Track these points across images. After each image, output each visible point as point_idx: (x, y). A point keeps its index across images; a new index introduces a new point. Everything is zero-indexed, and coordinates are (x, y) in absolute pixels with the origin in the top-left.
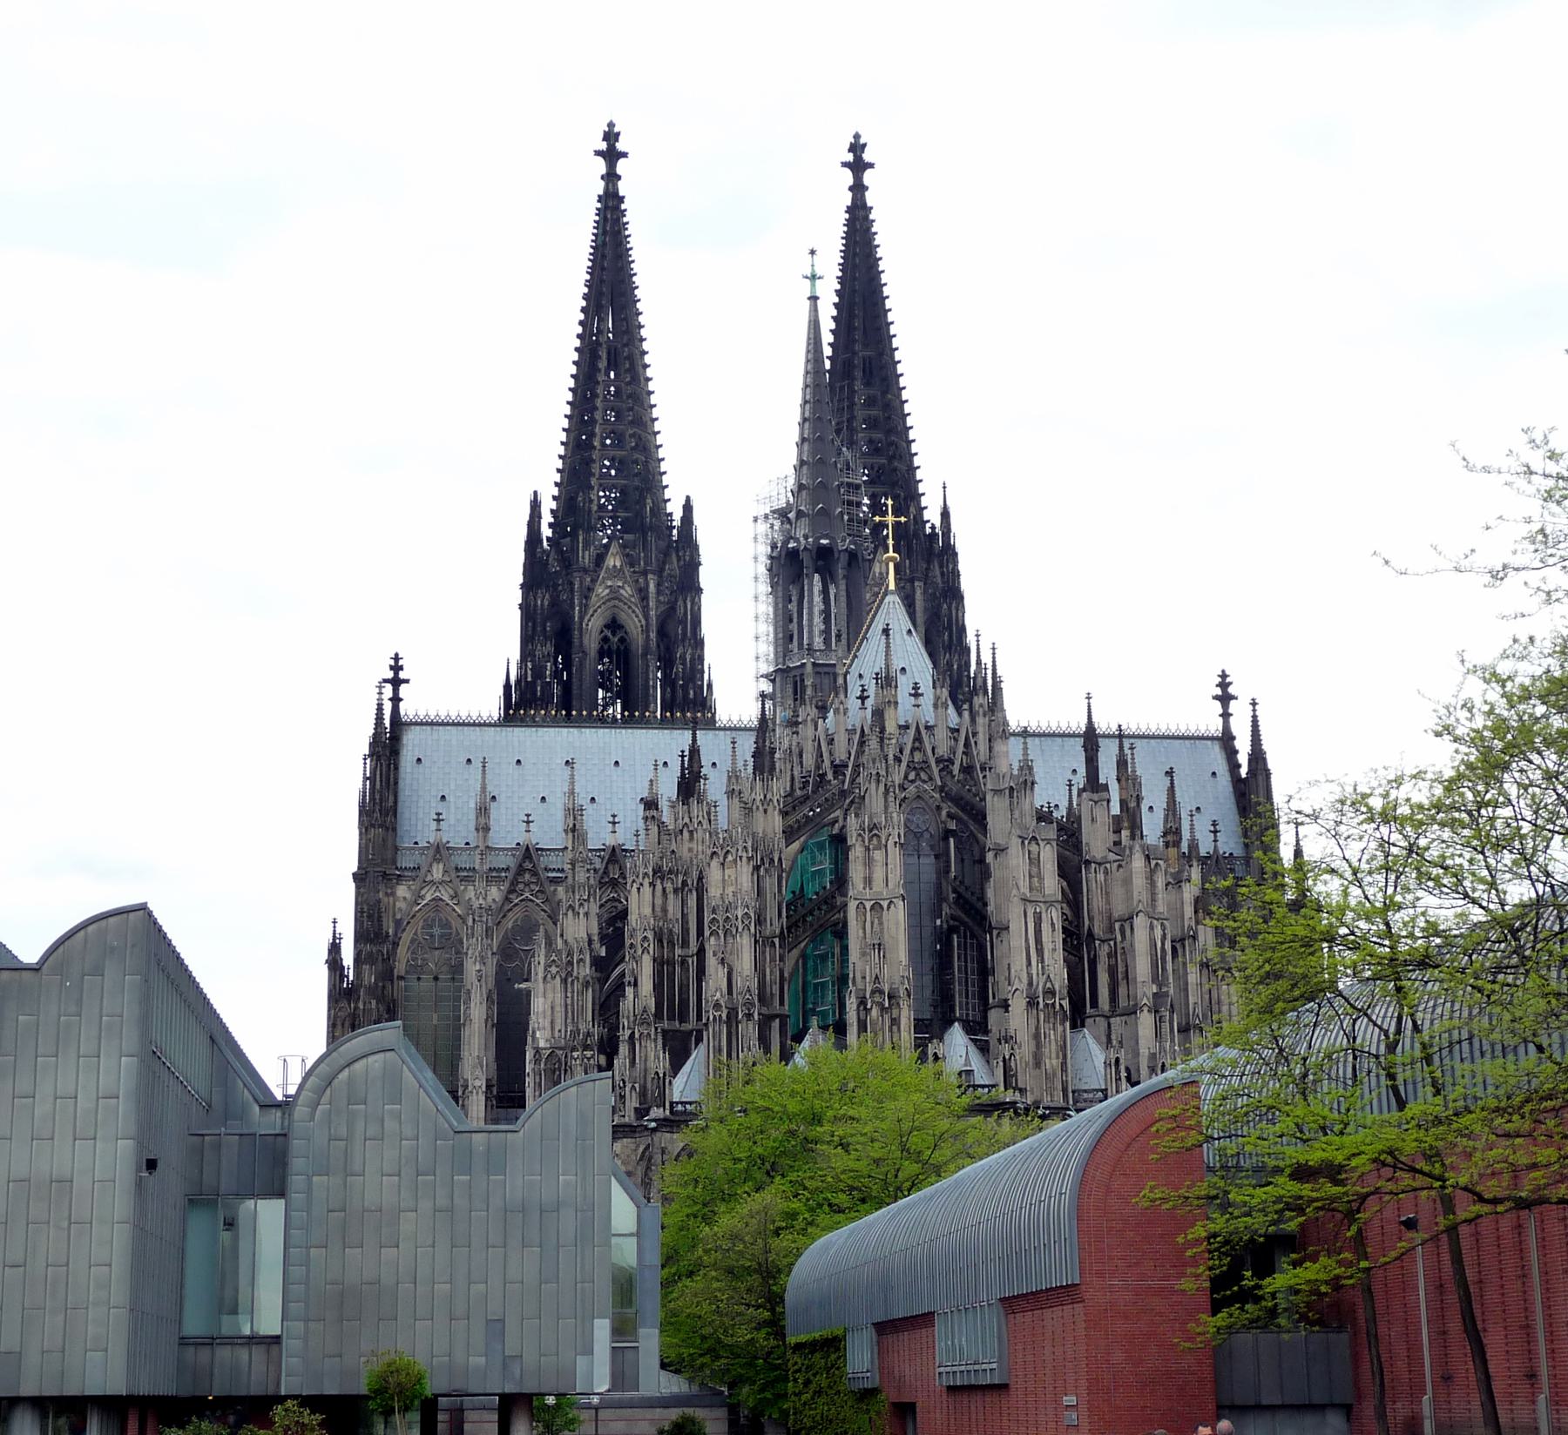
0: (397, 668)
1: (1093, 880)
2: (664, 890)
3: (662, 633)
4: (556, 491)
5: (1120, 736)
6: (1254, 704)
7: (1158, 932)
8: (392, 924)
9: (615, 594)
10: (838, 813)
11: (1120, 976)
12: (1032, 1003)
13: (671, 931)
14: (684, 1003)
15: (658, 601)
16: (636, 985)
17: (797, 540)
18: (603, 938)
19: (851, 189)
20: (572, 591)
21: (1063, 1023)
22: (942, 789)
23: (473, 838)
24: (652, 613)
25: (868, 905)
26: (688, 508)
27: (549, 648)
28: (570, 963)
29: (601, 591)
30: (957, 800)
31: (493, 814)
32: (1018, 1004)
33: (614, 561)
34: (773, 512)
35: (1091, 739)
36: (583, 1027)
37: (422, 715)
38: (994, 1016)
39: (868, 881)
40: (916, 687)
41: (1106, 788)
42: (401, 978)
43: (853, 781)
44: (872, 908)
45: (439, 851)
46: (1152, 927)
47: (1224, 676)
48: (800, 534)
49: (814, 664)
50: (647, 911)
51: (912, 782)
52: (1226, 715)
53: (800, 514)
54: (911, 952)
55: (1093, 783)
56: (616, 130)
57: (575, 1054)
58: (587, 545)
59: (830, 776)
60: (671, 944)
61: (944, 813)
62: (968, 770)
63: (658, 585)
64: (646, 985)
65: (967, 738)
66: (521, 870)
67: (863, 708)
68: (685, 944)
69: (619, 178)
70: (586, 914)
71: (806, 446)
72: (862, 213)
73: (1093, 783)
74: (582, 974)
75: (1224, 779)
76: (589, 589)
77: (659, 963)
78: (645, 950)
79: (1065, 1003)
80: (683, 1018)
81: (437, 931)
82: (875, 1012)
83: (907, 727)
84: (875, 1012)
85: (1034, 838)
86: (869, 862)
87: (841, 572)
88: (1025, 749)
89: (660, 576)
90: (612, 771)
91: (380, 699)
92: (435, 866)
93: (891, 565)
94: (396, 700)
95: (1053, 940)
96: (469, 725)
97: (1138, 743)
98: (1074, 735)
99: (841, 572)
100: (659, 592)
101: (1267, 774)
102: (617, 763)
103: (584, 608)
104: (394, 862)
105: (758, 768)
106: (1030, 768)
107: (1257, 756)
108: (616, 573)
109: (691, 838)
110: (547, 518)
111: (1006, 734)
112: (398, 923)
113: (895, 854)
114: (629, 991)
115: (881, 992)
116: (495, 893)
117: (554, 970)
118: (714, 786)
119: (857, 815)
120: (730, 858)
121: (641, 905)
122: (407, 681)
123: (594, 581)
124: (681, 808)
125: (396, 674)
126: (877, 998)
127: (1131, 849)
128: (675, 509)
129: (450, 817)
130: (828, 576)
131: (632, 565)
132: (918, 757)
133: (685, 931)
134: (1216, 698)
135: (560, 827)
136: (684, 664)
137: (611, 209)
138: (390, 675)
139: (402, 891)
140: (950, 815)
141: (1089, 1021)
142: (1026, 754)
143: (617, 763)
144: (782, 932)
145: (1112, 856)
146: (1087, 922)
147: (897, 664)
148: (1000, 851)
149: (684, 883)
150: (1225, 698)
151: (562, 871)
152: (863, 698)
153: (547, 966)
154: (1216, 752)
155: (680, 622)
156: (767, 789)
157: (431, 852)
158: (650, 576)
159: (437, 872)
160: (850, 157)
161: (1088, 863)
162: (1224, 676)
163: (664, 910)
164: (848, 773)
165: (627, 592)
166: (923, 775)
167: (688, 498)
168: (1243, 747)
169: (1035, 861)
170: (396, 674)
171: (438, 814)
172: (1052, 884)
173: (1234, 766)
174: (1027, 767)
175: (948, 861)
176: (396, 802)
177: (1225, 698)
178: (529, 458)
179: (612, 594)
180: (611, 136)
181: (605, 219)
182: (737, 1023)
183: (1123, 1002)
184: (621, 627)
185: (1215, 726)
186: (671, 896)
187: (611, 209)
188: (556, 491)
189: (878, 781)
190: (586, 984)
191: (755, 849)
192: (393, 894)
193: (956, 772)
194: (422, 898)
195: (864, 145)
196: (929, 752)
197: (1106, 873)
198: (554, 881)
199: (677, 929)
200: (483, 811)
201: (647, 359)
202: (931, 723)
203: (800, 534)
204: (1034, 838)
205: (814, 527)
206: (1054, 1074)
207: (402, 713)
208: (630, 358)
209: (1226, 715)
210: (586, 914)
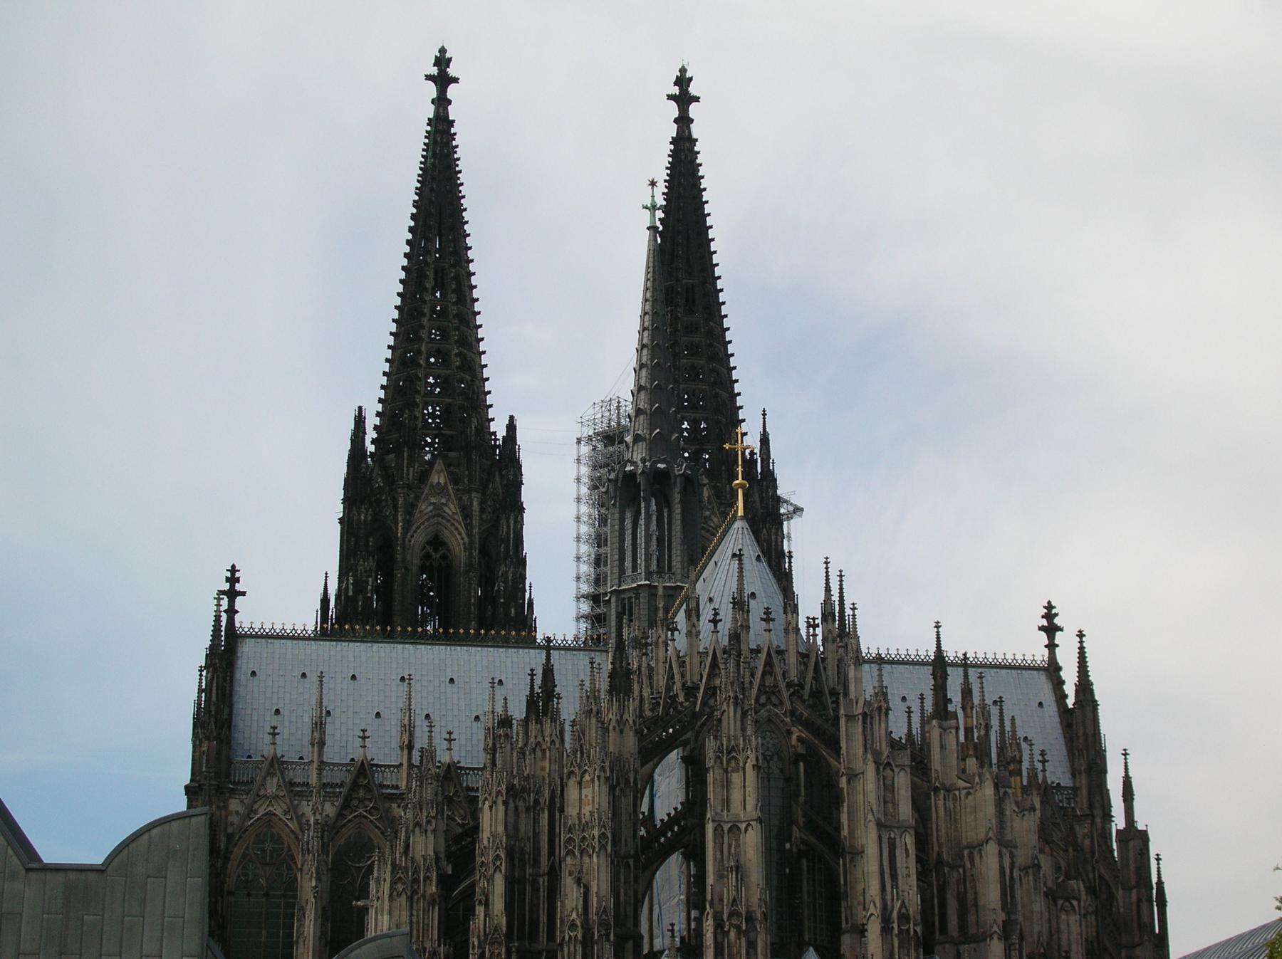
0: (233, 580)
1: (939, 804)
2: (516, 808)
3: (484, 551)
4: (379, 408)
5: (965, 664)
6: (1081, 635)
7: (1007, 860)
8: (223, 839)
9: (438, 511)
10: (689, 735)
11: (968, 903)
12: (886, 929)
13: (522, 851)
14: (535, 923)
15: (481, 519)
16: (487, 905)
17: (634, 463)
18: (449, 856)
19: (676, 121)
20: (395, 507)
21: (916, 950)
23: (309, 754)
24: (476, 531)
25: (726, 827)
26: (511, 427)
27: (371, 563)
28: (416, 881)
29: (425, 507)
30: (808, 725)
31: (329, 729)
32: (874, 929)
33: (439, 477)
34: (597, 434)
35: (939, 664)
36: (427, 945)
37: (257, 626)
38: (846, 941)
39: (727, 803)
40: (767, 612)
41: (955, 715)
42: (230, 893)
43: (704, 703)
44: (730, 830)
45: (276, 764)
46: (1001, 855)
47: (1049, 607)
48: (637, 457)
49: (665, 588)
50: (501, 829)
51: (764, 705)
52: (1052, 646)
53: (637, 438)
54: (768, 878)
55: (942, 709)
56: (448, 55)
58: (412, 461)
59: (681, 698)
61: (794, 737)
62: (817, 694)
63: (482, 503)
64: (498, 905)
65: (817, 664)
66: (355, 785)
67: (716, 631)
68: (536, 862)
69: (450, 102)
70: (434, 831)
71: (644, 372)
72: (687, 144)
73: (942, 709)
75: (1051, 709)
76: (413, 506)
77: (510, 882)
78: (497, 868)
79: (919, 929)
80: (533, 938)
81: (268, 846)
82: (732, 935)
83: (758, 651)
84: (732, 935)
85: (889, 764)
86: (727, 784)
87: (677, 497)
88: (880, 676)
89: (484, 495)
90: (448, 692)
91: (218, 611)
92: (269, 780)
93: (740, 492)
94: (232, 612)
95: (907, 865)
96: (293, 638)
97: (988, 673)
98: (922, 663)
99: (677, 497)
100: (482, 510)
101: (1094, 705)
102: (452, 681)
103: (408, 525)
104: (228, 776)
105: (613, 690)
106: (885, 695)
107: (1084, 686)
108: (441, 490)
110: (371, 434)
111: (859, 660)
112: (230, 837)
113: (751, 774)
114: (480, 910)
115: (739, 915)
116: (330, 809)
117: (400, 887)
118: (569, 707)
119: (716, 738)
120: (587, 777)
121: (492, 822)
122: (243, 594)
123: (417, 498)
124: (533, 727)
125: (232, 586)
126: (735, 921)
127: (980, 776)
128: (499, 428)
129: (285, 731)
130: (664, 501)
131: (456, 484)
132: (769, 681)
133: (537, 849)
134: (1041, 628)
135: (395, 744)
136: (506, 582)
137: (441, 134)
138: (227, 586)
139: (235, 805)
140: (800, 739)
141: (938, 948)
142: (881, 681)
143: (452, 681)
144: (636, 852)
145: (961, 783)
146: (936, 848)
147: (748, 590)
148: (852, 776)
149: (536, 802)
150: (1051, 629)
151: (397, 787)
152: (715, 622)
153: (393, 884)
154: (1042, 680)
155: (503, 541)
156: (622, 709)
157: (265, 766)
158: (474, 494)
159: (272, 786)
160: (676, 90)
161: (936, 789)
162: (1049, 607)
163: (516, 829)
164: (700, 695)
165: (451, 509)
166: (774, 699)
167: (512, 418)
168: (1070, 676)
169: (888, 788)
170: (232, 586)
171: (274, 728)
172: (905, 810)
173: (1062, 697)
174: (882, 693)
175: (798, 785)
176: (231, 714)
177: (1051, 629)
178: (354, 376)
179: (440, 511)
180: (442, 61)
181: (435, 142)
182: (592, 944)
183: (972, 930)
184: (443, 544)
185: (1041, 655)
186: (523, 815)
187: (441, 134)
188: (379, 408)
189: (736, 705)
190: (432, 903)
191: (612, 771)
192: (226, 808)
193: (806, 697)
194: (256, 812)
195: (691, 79)
196: (780, 677)
198: (391, 798)
199: (528, 848)
200: (319, 725)
201: (474, 280)
202: (783, 647)
203: (637, 457)
204: (889, 764)
205: (651, 449)
207: (237, 625)
208: (457, 278)
209: (1052, 646)
210: (434, 831)
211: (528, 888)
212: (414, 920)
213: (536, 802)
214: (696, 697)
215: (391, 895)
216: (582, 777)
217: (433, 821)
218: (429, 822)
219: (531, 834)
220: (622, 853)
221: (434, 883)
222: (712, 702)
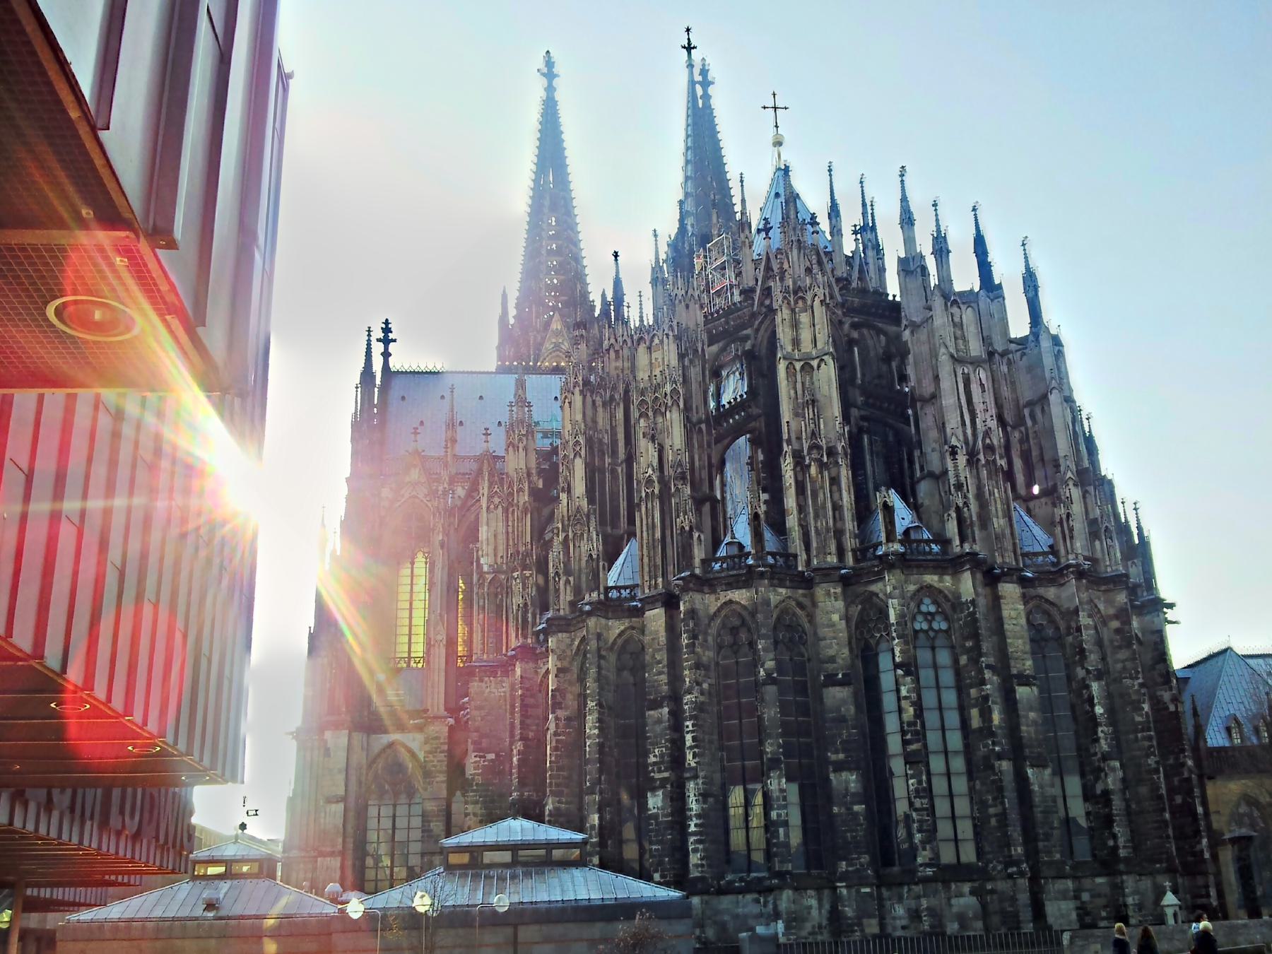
2: (594, 402)
13: (600, 441)
22: (843, 305)
109: (617, 357)
149: (612, 398)
186: (600, 410)
197: (1009, 363)
206: (1004, 535)
213: (612, 398)
220: (694, 419)
222: (767, 302)
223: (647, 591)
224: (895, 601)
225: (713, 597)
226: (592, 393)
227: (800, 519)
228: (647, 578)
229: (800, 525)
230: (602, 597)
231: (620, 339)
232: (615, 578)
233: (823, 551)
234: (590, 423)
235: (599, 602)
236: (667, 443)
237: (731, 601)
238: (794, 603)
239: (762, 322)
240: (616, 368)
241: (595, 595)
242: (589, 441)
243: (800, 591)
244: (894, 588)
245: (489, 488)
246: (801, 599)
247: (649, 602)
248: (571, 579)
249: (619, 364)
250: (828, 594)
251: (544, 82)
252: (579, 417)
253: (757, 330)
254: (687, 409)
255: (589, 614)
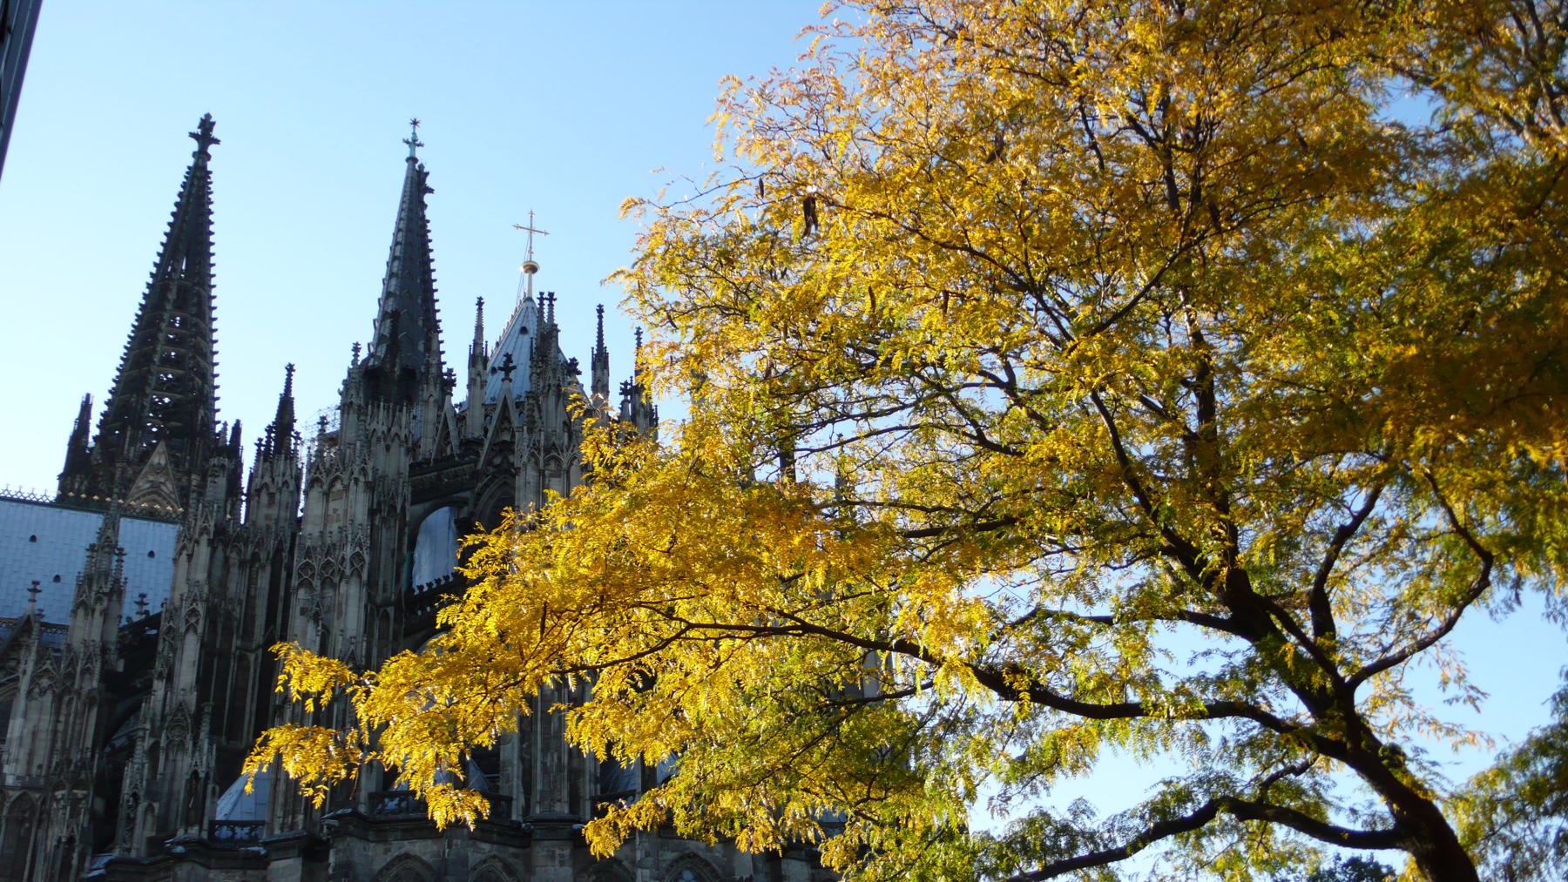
2: (227, 559)
13: (229, 616)
28: (70, 676)
57: (59, 794)
60: (228, 633)
64: (187, 675)
68: (247, 634)
74: (86, 687)
78: (191, 628)
109: (271, 503)
117: (45, 682)
120: (338, 486)
133: (250, 617)
149: (255, 557)
163: (223, 584)
186: (235, 570)
199: (238, 613)
211: (233, 665)
212: (61, 727)
213: (255, 557)
214: (478, 454)
215: (30, 692)
216: (332, 485)
217: (105, 600)
218: (99, 599)
219: (243, 597)
220: (379, 600)
221: (97, 676)
223: (277, 832)
224: (647, 872)
225: (380, 848)
226: (226, 546)
227: (521, 750)
228: (279, 813)
229: (522, 759)
230: (205, 835)
231: (279, 480)
232: (226, 811)
233: (550, 796)
234: (218, 587)
235: (200, 842)
236: (336, 626)
237: (407, 856)
238: (499, 865)
239: (486, 485)
240: (268, 517)
241: (194, 831)
242: (212, 613)
243: (512, 850)
244: (647, 854)
245: (36, 663)
246: (511, 860)
247: (279, 848)
248: (156, 805)
249: (274, 512)
250: (552, 857)
251: (194, 146)
252: (201, 576)
253: (479, 495)
254: (371, 584)
255: (181, 858)
